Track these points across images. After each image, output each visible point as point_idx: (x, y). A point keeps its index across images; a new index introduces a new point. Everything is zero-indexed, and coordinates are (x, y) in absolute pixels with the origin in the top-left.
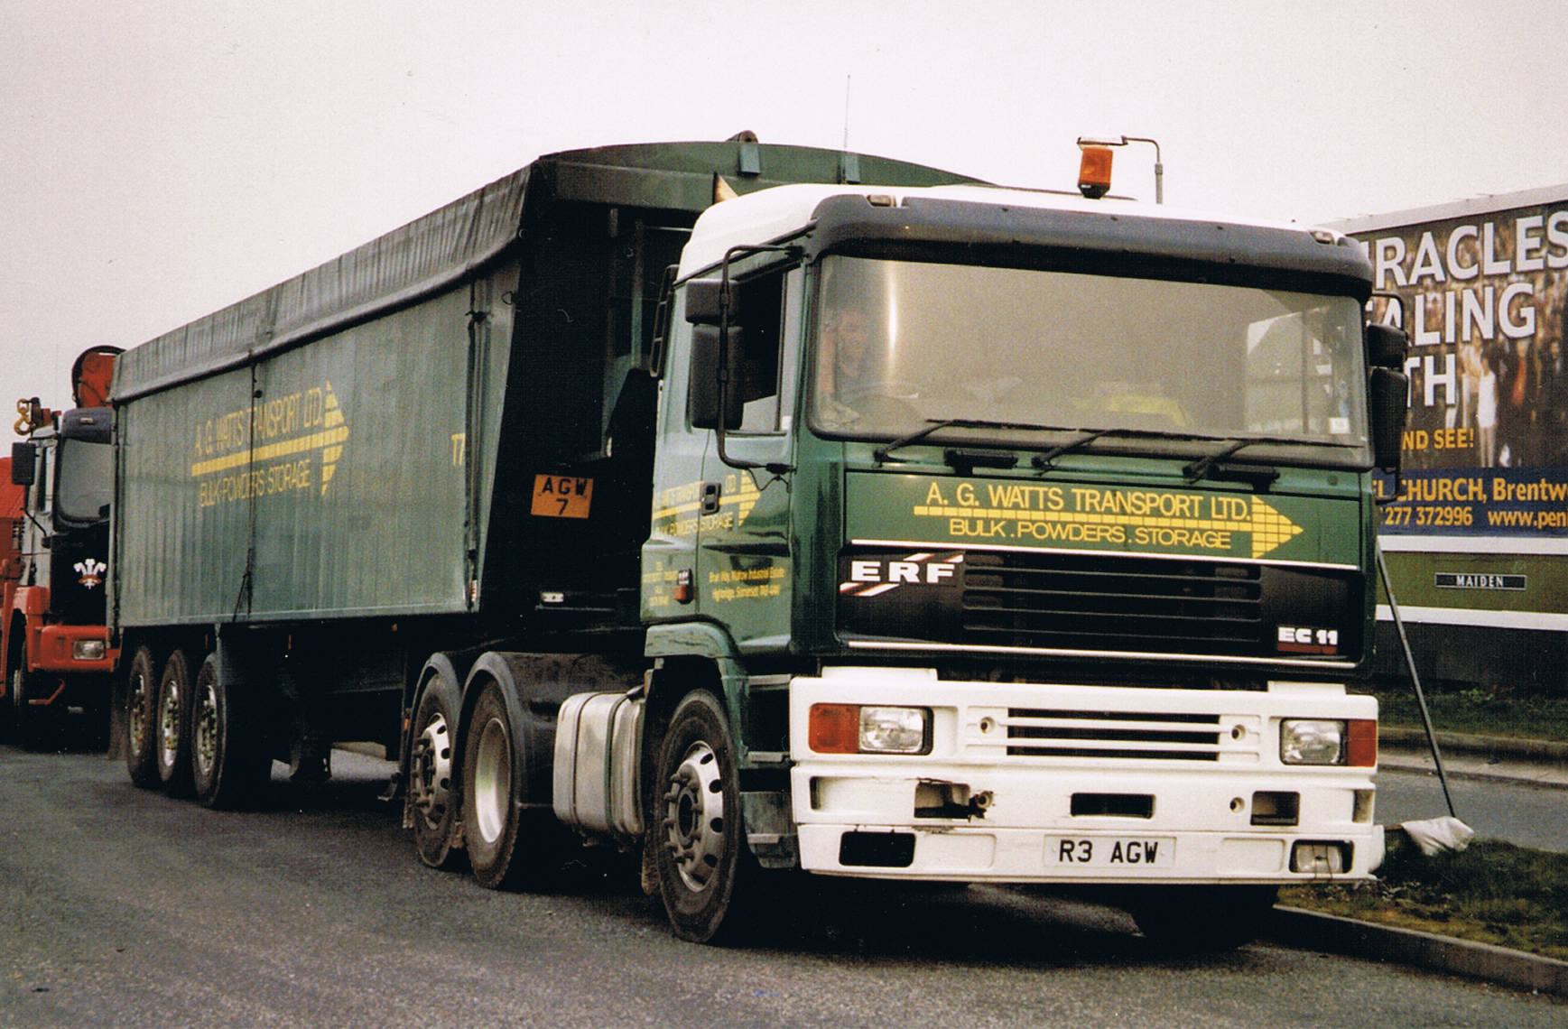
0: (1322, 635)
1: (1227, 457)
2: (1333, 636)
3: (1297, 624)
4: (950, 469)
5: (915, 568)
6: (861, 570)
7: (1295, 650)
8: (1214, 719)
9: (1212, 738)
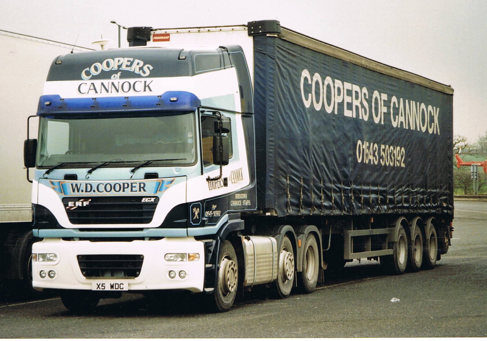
5: (81, 203)
6: (70, 204)
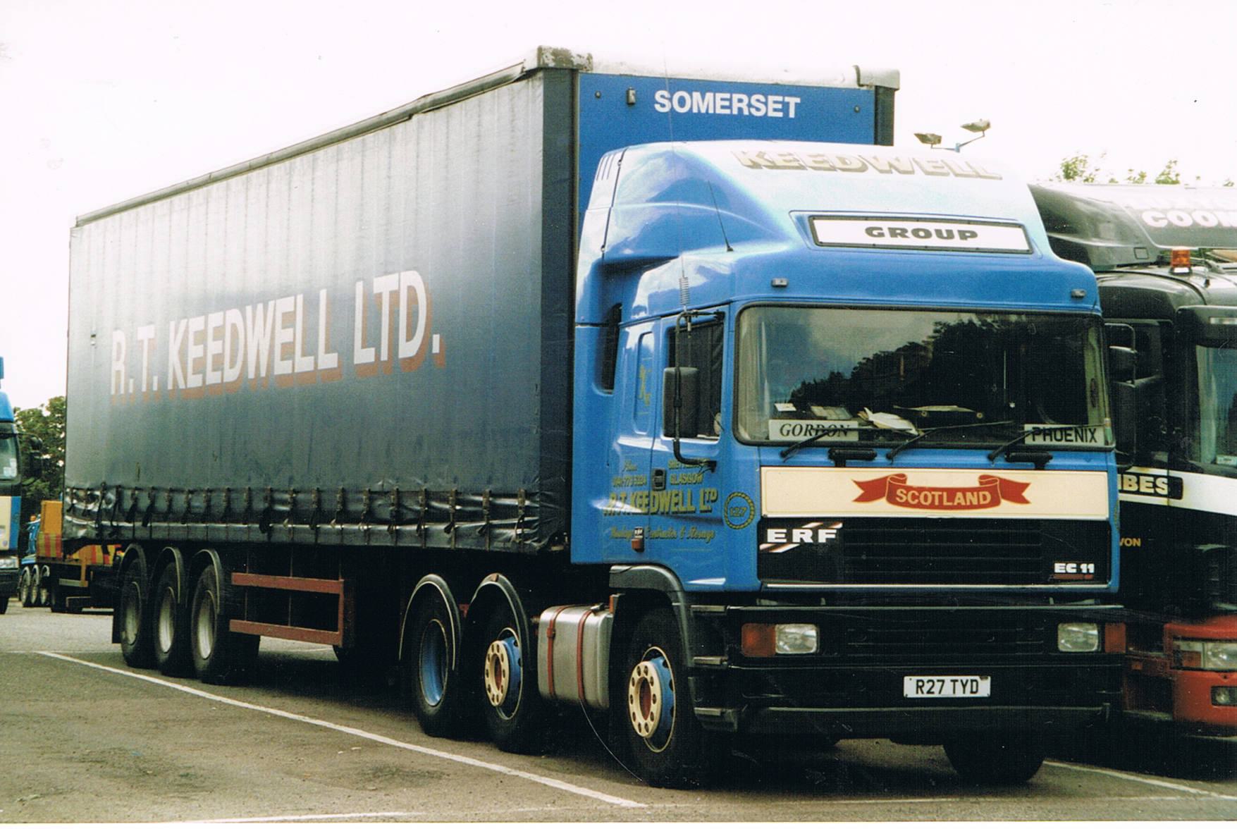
0: (1084, 567)
2: (1091, 567)
3: (1066, 560)
5: (810, 533)
6: (773, 535)
7: (1066, 578)
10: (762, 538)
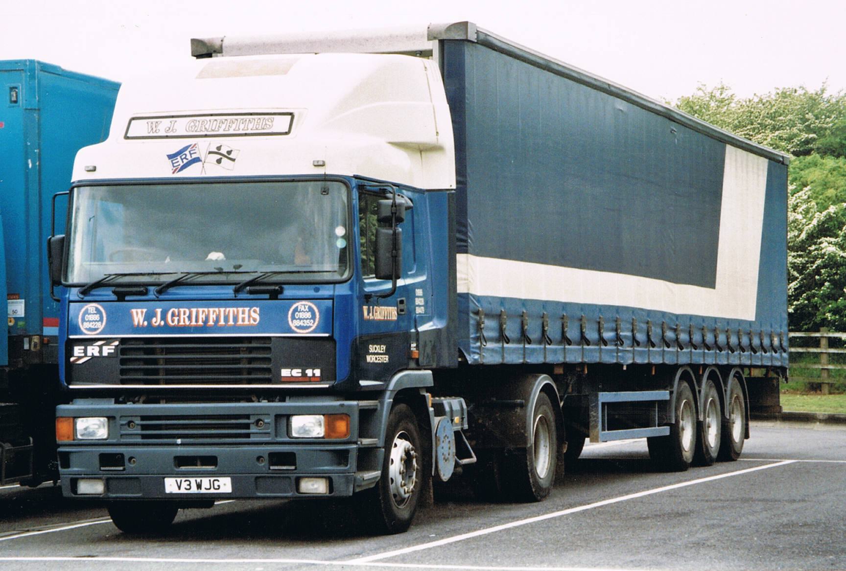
0: (309, 372)
1: (252, 283)
2: (318, 372)
3: (292, 366)
4: (114, 297)
5: (97, 349)
6: (78, 351)
7: (291, 380)
8: (247, 417)
9: (247, 426)
10: (70, 353)
